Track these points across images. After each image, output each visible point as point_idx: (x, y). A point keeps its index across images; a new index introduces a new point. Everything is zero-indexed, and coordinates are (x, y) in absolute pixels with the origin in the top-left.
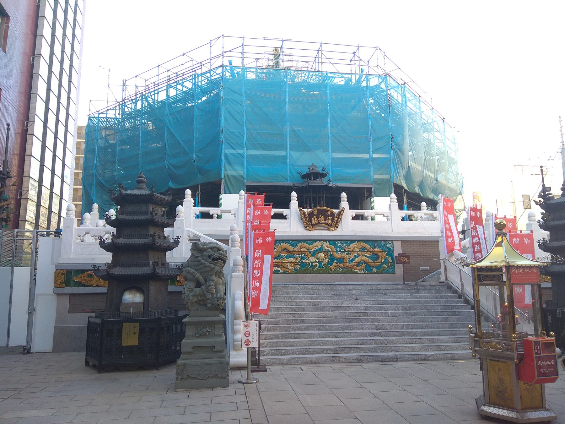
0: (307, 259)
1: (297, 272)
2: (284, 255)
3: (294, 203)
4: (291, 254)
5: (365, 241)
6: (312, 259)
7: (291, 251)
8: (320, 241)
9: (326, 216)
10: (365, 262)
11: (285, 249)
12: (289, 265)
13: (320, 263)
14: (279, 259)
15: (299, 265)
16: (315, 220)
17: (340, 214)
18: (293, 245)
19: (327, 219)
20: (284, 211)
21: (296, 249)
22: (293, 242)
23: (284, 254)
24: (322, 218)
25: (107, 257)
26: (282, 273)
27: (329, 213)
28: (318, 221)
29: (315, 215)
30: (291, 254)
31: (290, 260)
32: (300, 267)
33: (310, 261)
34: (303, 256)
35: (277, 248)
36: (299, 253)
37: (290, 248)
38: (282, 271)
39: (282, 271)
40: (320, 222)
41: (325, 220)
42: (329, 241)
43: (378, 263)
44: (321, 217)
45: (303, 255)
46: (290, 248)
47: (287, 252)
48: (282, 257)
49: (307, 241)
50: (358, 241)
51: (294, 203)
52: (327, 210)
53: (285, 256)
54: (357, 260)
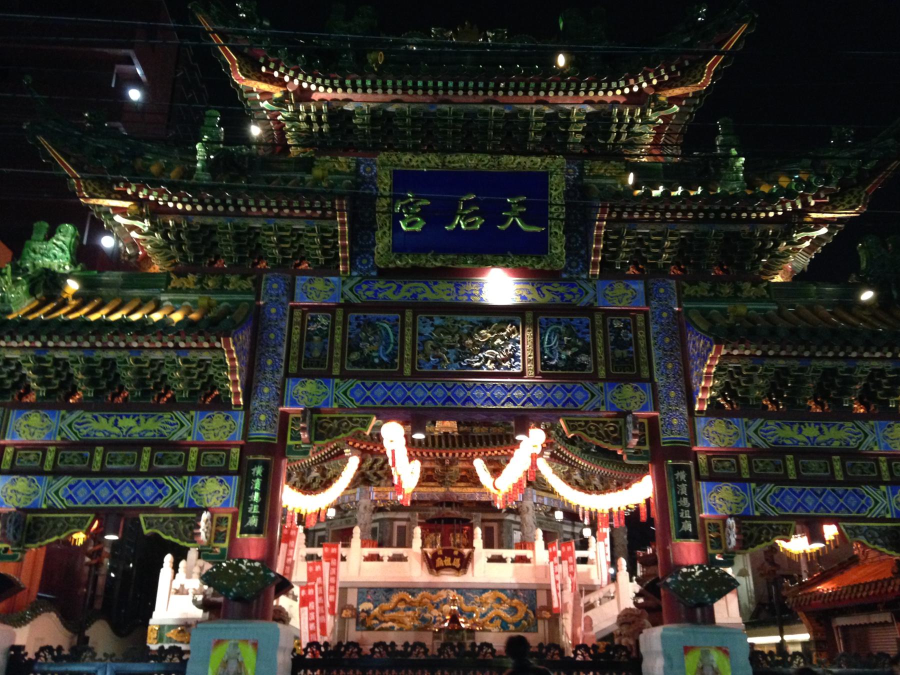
3: (417, 542)
4: (410, 606)
5: (503, 590)
6: (435, 612)
8: (446, 589)
10: (499, 617)
11: (402, 600)
12: (407, 620)
16: (439, 562)
17: (470, 555)
18: (413, 595)
22: (412, 589)
23: (402, 606)
24: (448, 561)
25: (199, 613)
27: (456, 553)
30: (410, 606)
31: (410, 613)
41: (452, 561)
42: (457, 589)
48: (399, 610)
50: (493, 590)
51: (417, 542)
54: (492, 614)
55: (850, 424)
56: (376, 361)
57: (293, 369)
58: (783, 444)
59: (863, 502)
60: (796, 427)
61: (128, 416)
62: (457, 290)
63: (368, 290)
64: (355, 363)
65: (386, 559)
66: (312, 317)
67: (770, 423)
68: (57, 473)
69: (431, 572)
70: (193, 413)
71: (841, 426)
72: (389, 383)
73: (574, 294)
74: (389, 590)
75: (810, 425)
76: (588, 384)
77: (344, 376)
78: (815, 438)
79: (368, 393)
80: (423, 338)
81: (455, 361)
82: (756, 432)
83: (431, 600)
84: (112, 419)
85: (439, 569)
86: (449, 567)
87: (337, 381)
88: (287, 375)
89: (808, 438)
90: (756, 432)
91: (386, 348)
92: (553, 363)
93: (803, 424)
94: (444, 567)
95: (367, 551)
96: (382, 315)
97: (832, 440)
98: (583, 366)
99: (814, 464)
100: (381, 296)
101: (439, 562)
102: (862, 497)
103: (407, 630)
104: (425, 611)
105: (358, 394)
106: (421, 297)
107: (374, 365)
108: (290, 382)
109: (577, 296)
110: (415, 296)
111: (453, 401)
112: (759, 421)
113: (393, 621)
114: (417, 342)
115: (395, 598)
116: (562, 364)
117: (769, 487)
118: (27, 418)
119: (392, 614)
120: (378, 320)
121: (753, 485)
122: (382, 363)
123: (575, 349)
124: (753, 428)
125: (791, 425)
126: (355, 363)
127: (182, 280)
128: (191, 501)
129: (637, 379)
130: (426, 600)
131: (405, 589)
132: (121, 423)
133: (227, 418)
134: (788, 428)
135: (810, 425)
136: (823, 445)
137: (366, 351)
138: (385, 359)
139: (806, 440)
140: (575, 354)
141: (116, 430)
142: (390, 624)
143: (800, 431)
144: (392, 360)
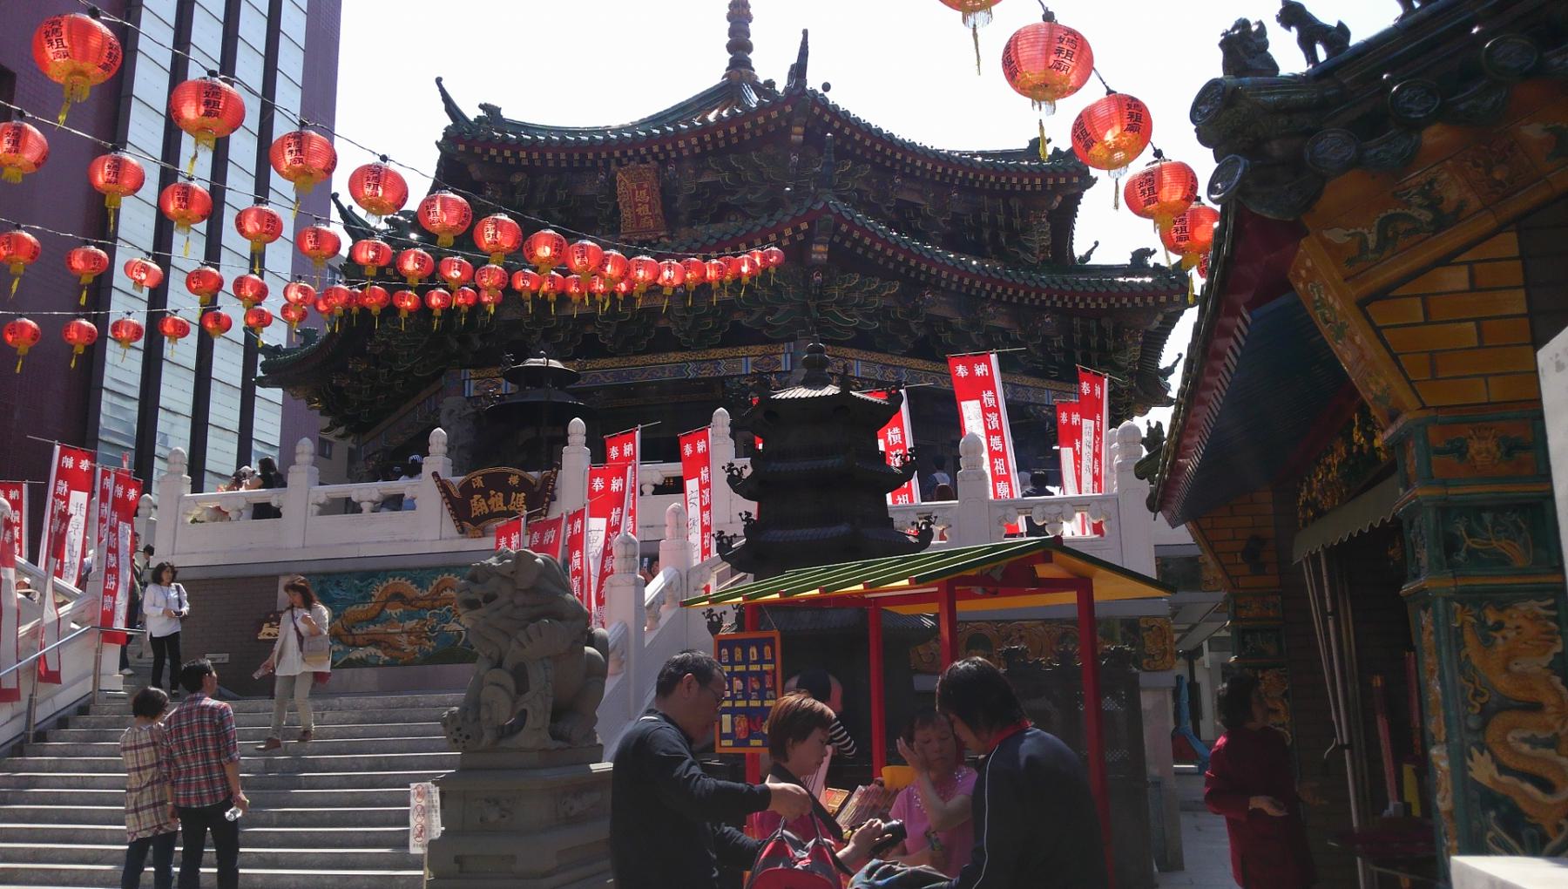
0: (454, 621)
1: (430, 659)
2: (393, 612)
3: (437, 459)
7: (413, 600)
9: (508, 491)
11: (398, 597)
12: (404, 639)
14: (381, 623)
15: (435, 639)
16: (478, 505)
18: (421, 584)
19: (513, 499)
20: (402, 485)
21: (426, 593)
22: (422, 571)
23: (394, 611)
24: (497, 501)
26: (386, 664)
27: (514, 480)
28: (489, 506)
29: (478, 490)
32: (435, 644)
33: (463, 626)
34: (444, 613)
35: (377, 594)
37: (411, 589)
38: (387, 658)
39: (387, 658)
40: (495, 510)
44: (494, 496)
45: (444, 609)
46: (411, 589)
47: (403, 602)
48: (389, 619)
49: (458, 570)
52: (509, 475)
53: (396, 614)
65: (366, 506)
101: (478, 505)
103: (404, 664)
113: (376, 643)
115: (379, 590)
119: (372, 627)
142: (371, 650)
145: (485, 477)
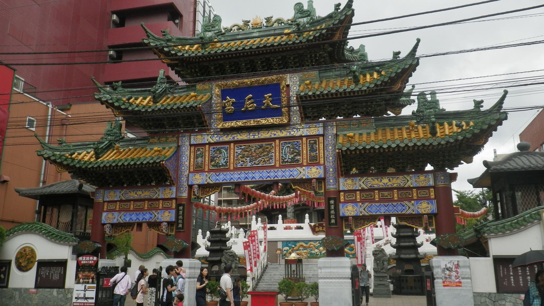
1: (309, 258)
3: (307, 220)
4: (305, 248)
6: (316, 251)
11: (302, 246)
12: (304, 254)
13: (320, 253)
16: (317, 229)
18: (306, 244)
22: (307, 241)
24: (321, 228)
36: (309, 247)
37: (305, 245)
43: (353, 252)
46: (305, 245)
48: (300, 250)
51: (307, 220)
55: (402, 177)
56: (221, 164)
57: (192, 170)
58: (374, 186)
59: (404, 208)
60: (379, 180)
61: (139, 191)
62: (250, 134)
63: (217, 137)
64: (213, 166)
66: (198, 149)
67: (369, 178)
68: (120, 211)
69: (314, 234)
70: (159, 188)
71: (398, 178)
72: (225, 173)
73: (295, 132)
74: (295, 242)
75: (385, 178)
76: (299, 168)
77: (210, 171)
78: (387, 183)
79: (217, 177)
80: (237, 154)
81: (249, 162)
82: (363, 183)
83: (314, 246)
84: (135, 192)
85: (317, 232)
86: (321, 231)
87: (206, 173)
88: (190, 172)
89: (384, 183)
90: (363, 183)
91: (224, 159)
92: (286, 160)
93: (383, 178)
94: (320, 231)
95: (285, 225)
96: (222, 146)
97: (394, 184)
98: (298, 161)
99: (386, 193)
100: (221, 139)
101: (317, 229)
102: (404, 206)
104: (312, 250)
105: (214, 178)
106: (236, 138)
107: (220, 166)
108: (191, 175)
109: (296, 132)
110: (234, 138)
111: (248, 178)
112: (365, 178)
114: (235, 156)
115: (298, 244)
116: (290, 160)
117: (366, 204)
118: (109, 193)
120: (221, 148)
121: (360, 204)
122: (223, 165)
123: (295, 154)
124: (362, 181)
125: (377, 179)
126: (213, 166)
127: (154, 139)
128: (161, 219)
129: (318, 164)
130: (312, 246)
131: (303, 241)
132: (137, 193)
133: (170, 189)
134: (376, 180)
135: (385, 178)
136: (390, 186)
137: (217, 161)
138: (224, 164)
139: (383, 184)
140: (296, 156)
141: (136, 196)
143: (381, 180)
144: (226, 164)
145: (319, 224)
